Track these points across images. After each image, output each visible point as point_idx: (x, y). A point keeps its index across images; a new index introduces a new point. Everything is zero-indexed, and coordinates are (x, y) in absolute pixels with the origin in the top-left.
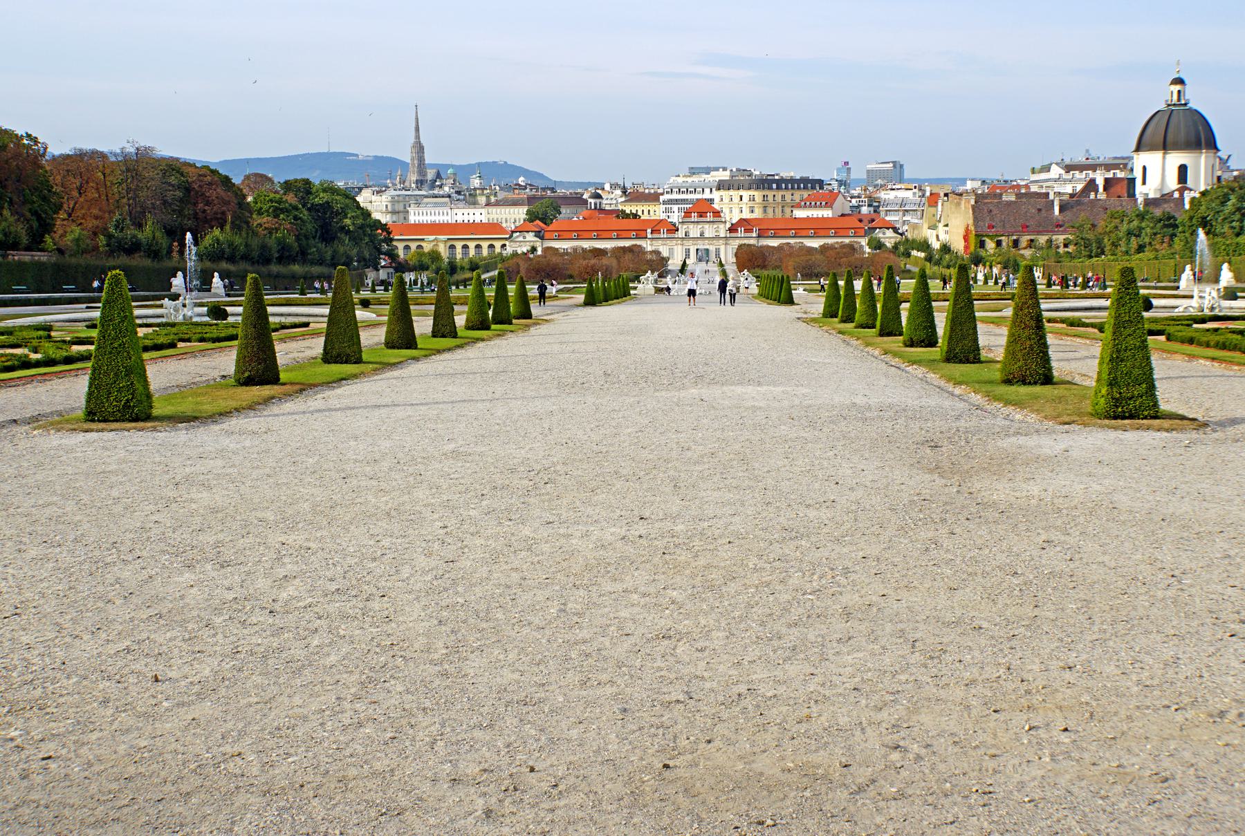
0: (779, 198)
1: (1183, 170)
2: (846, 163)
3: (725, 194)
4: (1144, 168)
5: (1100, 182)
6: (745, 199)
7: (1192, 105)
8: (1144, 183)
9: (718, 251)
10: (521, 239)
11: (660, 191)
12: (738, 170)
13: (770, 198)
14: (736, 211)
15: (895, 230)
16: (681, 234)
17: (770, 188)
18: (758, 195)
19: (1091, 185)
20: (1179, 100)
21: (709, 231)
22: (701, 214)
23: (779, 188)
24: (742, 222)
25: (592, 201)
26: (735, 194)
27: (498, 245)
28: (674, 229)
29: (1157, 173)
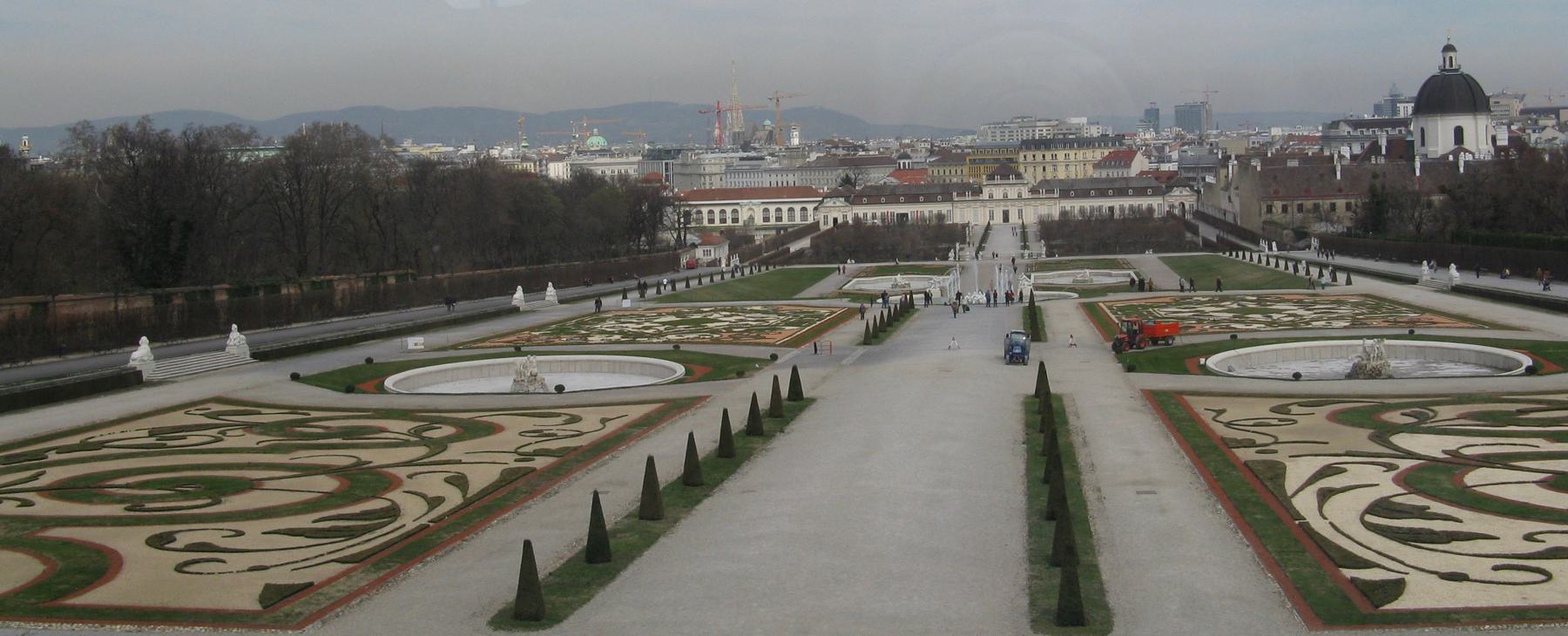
1: (1459, 132)
3: (1030, 155)
5: (1383, 143)
6: (1048, 157)
7: (1465, 70)
8: (1423, 144)
9: (1020, 212)
13: (1072, 157)
15: (1192, 187)
16: (985, 195)
17: (1071, 147)
18: (1061, 155)
19: (1374, 148)
21: (1012, 193)
22: (1005, 176)
24: (1045, 182)
26: (1039, 155)
27: (810, 207)
28: (977, 191)
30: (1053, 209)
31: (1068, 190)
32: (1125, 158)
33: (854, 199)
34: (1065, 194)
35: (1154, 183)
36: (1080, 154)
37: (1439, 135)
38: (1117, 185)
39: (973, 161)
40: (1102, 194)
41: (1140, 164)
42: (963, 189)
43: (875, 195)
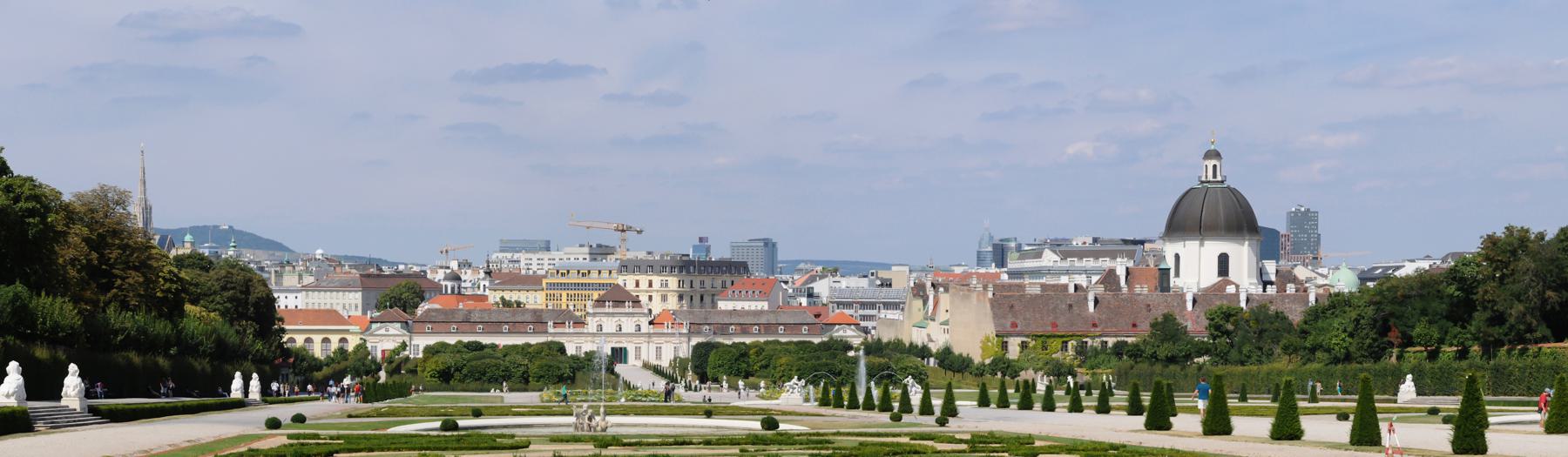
1: (1223, 261)
2: (701, 240)
4: (1177, 257)
5: (1121, 272)
6: (656, 285)
8: (1177, 274)
9: (638, 349)
10: (383, 331)
11: (541, 272)
12: (599, 246)
14: (657, 298)
20: (1215, 176)
21: (629, 325)
22: (619, 303)
25: (449, 284)
28: (580, 323)
29: (1195, 266)
38: (763, 320)
39: (552, 286)
42: (562, 318)
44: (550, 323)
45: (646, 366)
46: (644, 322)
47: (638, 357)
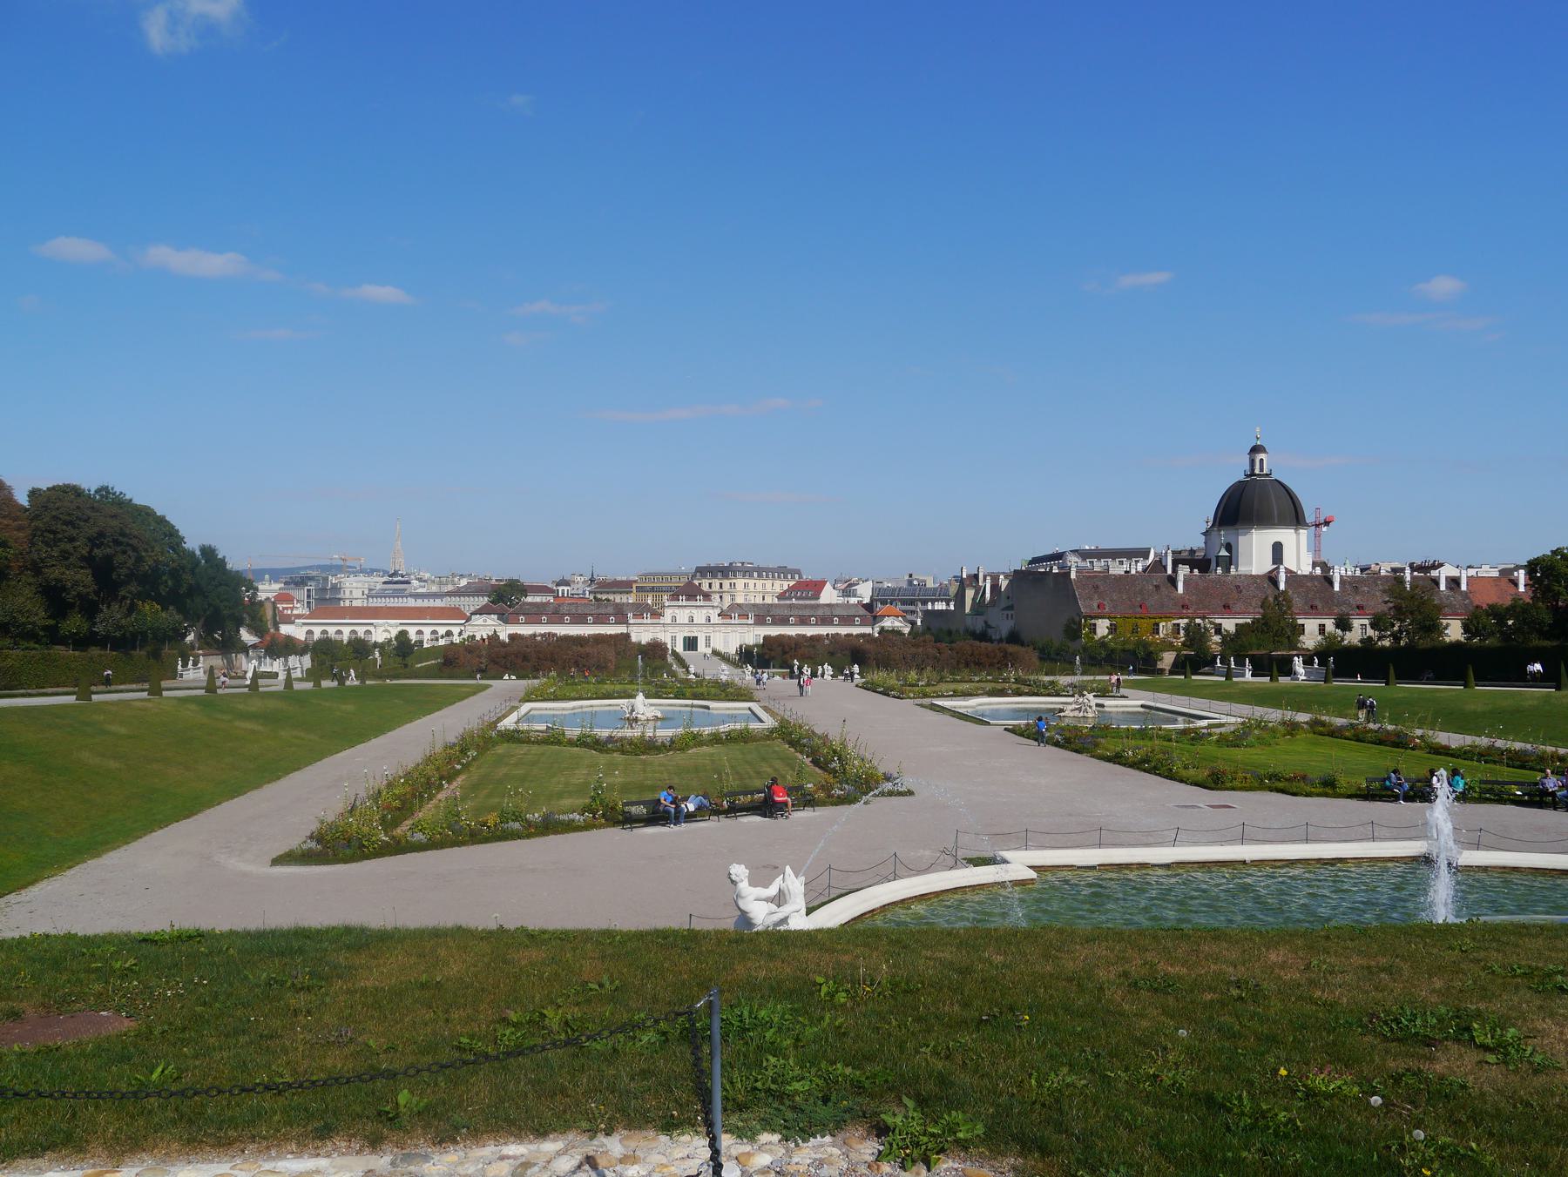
0: (759, 588)
1: (1277, 549)
9: (708, 639)
10: (480, 622)
13: (751, 586)
16: (667, 619)
17: (751, 576)
18: (740, 582)
21: (700, 616)
23: (760, 576)
24: (734, 607)
28: (657, 614)
30: (753, 635)
31: (762, 615)
32: (817, 586)
33: (505, 619)
34: (760, 621)
35: (863, 612)
36: (760, 583)
37: (1255, 551)
38: (820, 612)
40: (803, 621)
41: (829, 596)
42: (640, 610)
43: (534, 614)
44: (630, 615)
45: (715, 653)
46: (714, 614)
47: (708, 645)
